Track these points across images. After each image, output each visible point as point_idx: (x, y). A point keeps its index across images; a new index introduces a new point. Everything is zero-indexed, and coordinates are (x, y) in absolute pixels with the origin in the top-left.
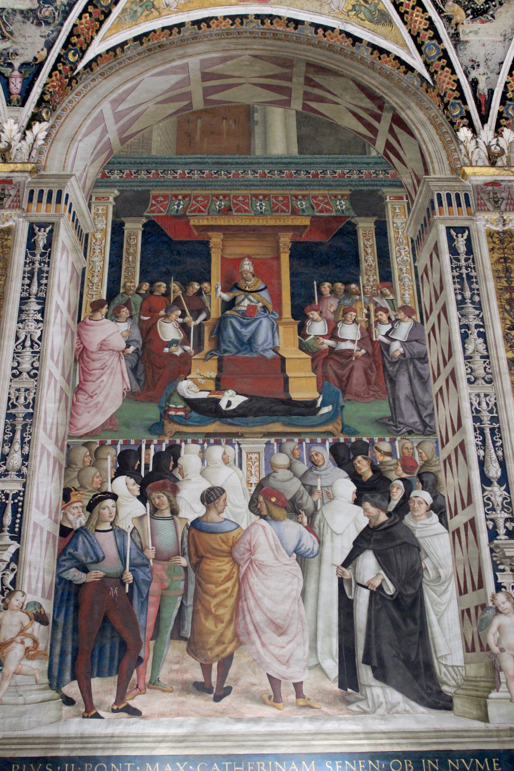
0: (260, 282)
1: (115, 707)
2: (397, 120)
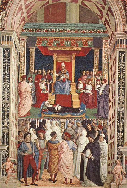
2: (110, 9)
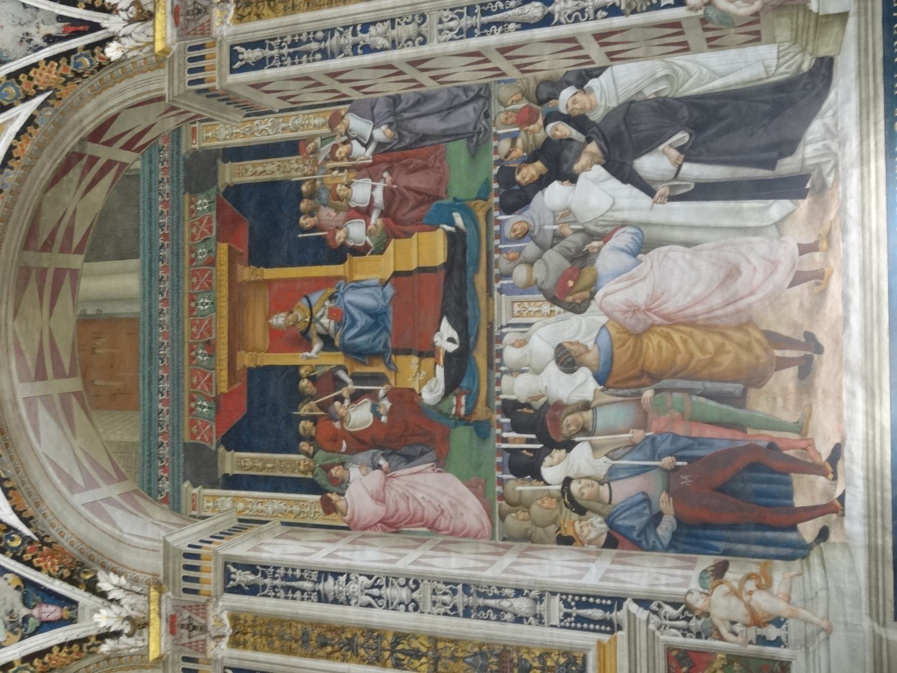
0: (299, 303)
1: (831, 476)
2: (96, 135)
